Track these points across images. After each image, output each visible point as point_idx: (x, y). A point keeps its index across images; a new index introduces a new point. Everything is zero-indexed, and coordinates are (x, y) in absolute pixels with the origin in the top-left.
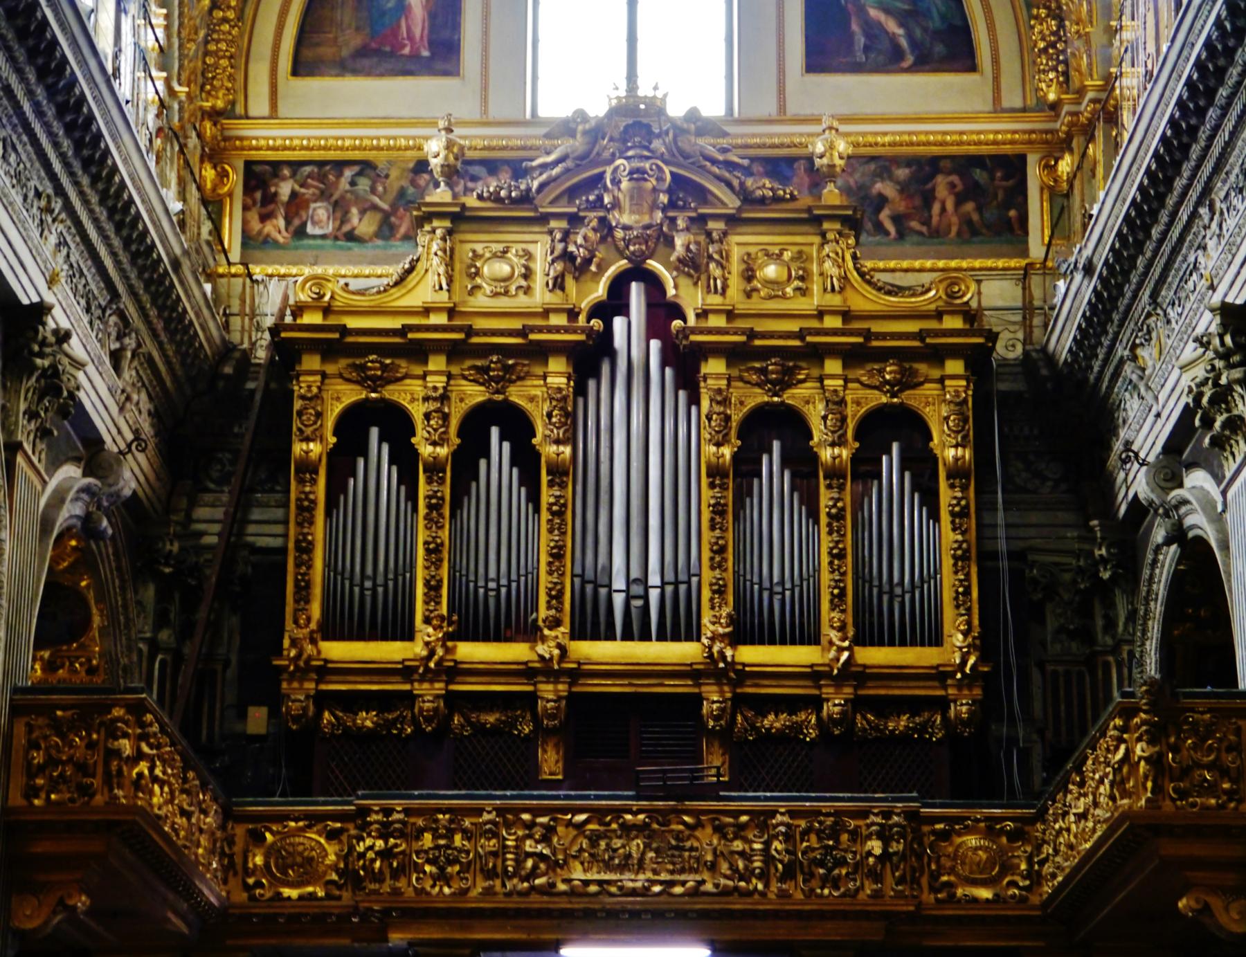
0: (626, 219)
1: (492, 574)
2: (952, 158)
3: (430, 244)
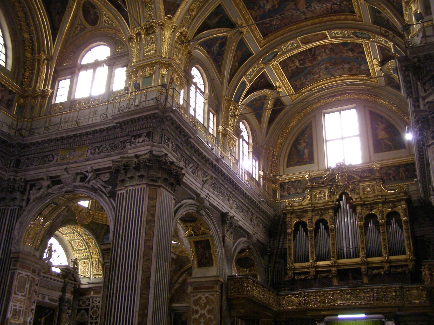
0: (340, 184)
2: (403, 165)
3: (307, 193)
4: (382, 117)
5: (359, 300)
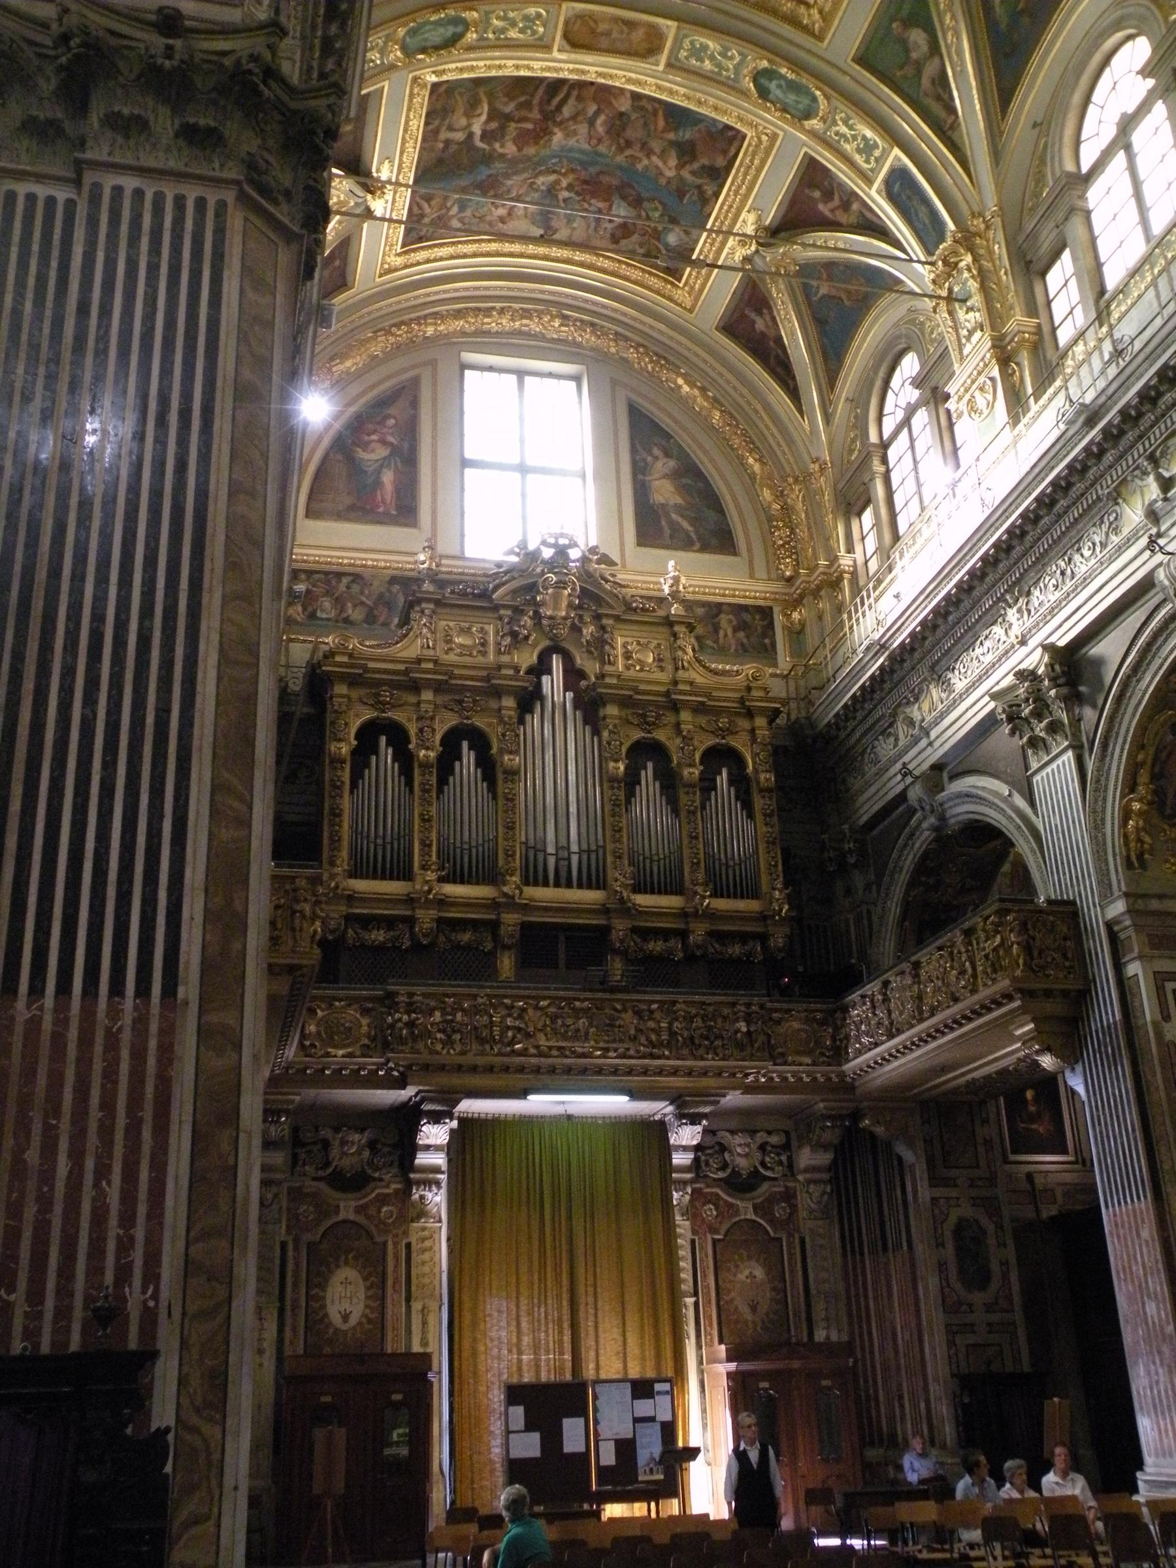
1: (466, 838)
4: (668, 436)
5: (621, 1041)
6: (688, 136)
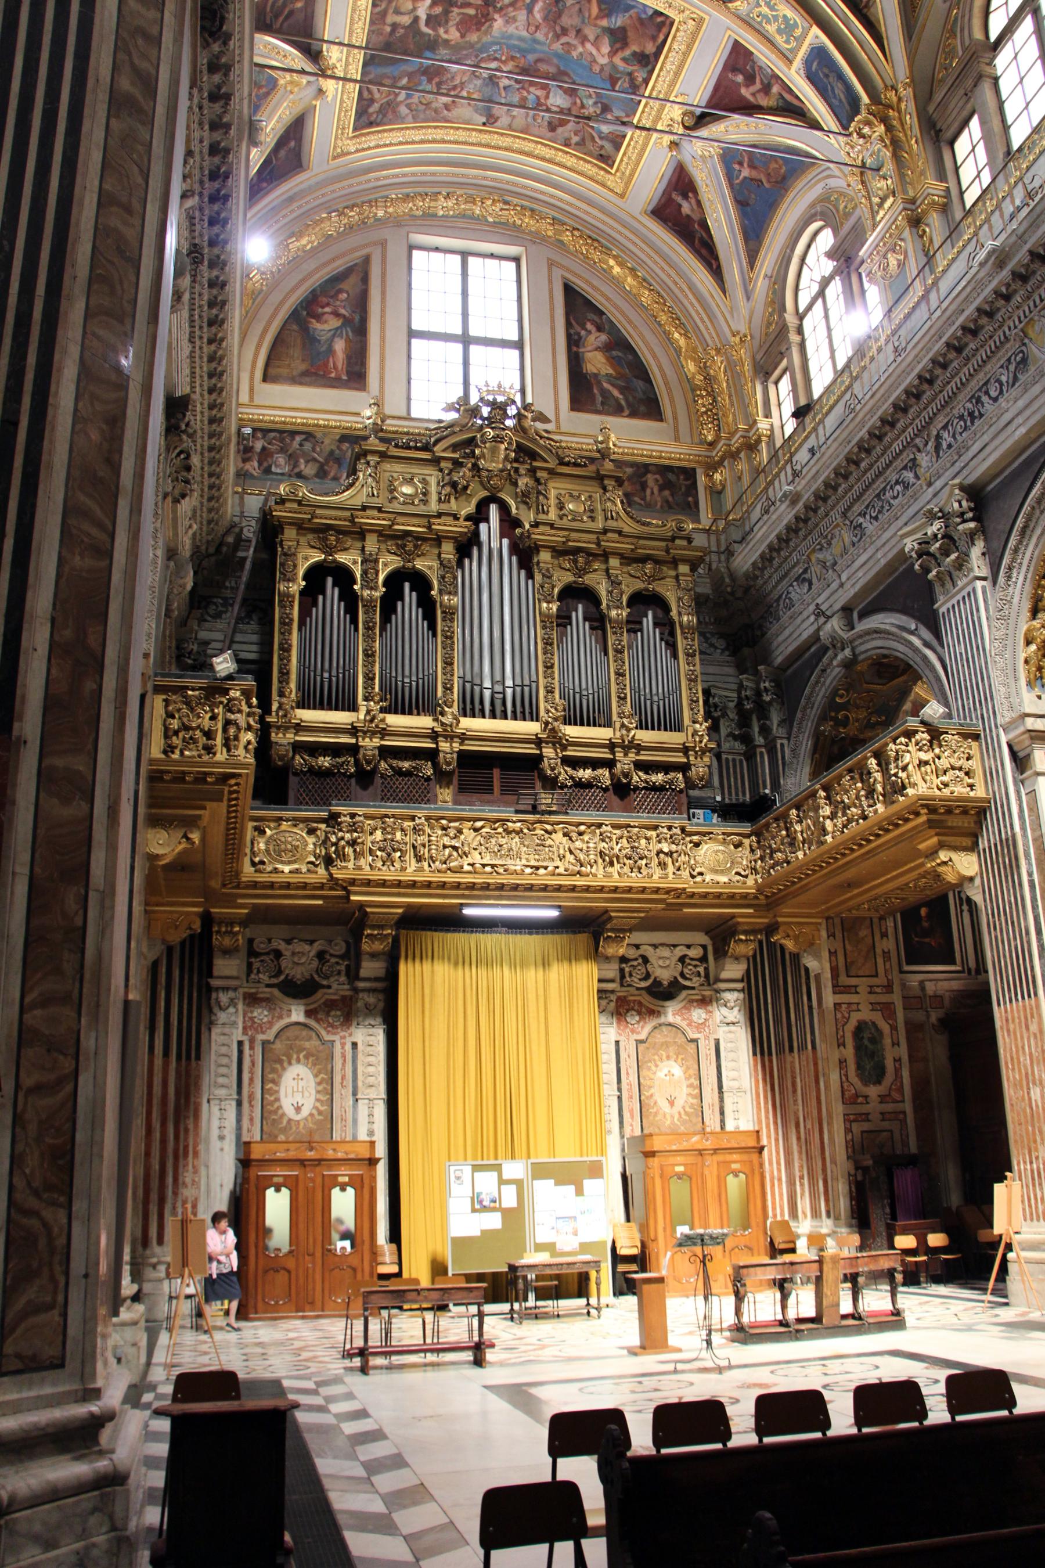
6: (619, 23)
